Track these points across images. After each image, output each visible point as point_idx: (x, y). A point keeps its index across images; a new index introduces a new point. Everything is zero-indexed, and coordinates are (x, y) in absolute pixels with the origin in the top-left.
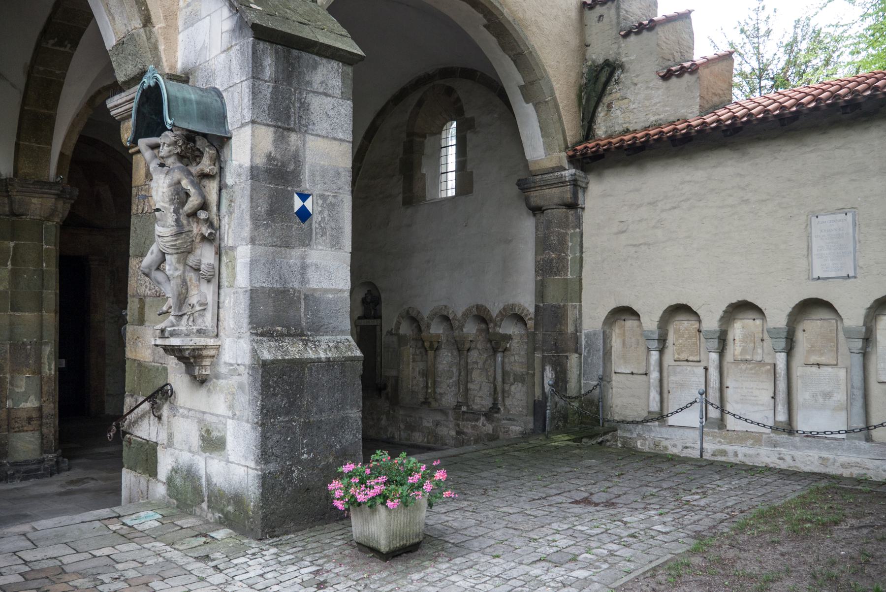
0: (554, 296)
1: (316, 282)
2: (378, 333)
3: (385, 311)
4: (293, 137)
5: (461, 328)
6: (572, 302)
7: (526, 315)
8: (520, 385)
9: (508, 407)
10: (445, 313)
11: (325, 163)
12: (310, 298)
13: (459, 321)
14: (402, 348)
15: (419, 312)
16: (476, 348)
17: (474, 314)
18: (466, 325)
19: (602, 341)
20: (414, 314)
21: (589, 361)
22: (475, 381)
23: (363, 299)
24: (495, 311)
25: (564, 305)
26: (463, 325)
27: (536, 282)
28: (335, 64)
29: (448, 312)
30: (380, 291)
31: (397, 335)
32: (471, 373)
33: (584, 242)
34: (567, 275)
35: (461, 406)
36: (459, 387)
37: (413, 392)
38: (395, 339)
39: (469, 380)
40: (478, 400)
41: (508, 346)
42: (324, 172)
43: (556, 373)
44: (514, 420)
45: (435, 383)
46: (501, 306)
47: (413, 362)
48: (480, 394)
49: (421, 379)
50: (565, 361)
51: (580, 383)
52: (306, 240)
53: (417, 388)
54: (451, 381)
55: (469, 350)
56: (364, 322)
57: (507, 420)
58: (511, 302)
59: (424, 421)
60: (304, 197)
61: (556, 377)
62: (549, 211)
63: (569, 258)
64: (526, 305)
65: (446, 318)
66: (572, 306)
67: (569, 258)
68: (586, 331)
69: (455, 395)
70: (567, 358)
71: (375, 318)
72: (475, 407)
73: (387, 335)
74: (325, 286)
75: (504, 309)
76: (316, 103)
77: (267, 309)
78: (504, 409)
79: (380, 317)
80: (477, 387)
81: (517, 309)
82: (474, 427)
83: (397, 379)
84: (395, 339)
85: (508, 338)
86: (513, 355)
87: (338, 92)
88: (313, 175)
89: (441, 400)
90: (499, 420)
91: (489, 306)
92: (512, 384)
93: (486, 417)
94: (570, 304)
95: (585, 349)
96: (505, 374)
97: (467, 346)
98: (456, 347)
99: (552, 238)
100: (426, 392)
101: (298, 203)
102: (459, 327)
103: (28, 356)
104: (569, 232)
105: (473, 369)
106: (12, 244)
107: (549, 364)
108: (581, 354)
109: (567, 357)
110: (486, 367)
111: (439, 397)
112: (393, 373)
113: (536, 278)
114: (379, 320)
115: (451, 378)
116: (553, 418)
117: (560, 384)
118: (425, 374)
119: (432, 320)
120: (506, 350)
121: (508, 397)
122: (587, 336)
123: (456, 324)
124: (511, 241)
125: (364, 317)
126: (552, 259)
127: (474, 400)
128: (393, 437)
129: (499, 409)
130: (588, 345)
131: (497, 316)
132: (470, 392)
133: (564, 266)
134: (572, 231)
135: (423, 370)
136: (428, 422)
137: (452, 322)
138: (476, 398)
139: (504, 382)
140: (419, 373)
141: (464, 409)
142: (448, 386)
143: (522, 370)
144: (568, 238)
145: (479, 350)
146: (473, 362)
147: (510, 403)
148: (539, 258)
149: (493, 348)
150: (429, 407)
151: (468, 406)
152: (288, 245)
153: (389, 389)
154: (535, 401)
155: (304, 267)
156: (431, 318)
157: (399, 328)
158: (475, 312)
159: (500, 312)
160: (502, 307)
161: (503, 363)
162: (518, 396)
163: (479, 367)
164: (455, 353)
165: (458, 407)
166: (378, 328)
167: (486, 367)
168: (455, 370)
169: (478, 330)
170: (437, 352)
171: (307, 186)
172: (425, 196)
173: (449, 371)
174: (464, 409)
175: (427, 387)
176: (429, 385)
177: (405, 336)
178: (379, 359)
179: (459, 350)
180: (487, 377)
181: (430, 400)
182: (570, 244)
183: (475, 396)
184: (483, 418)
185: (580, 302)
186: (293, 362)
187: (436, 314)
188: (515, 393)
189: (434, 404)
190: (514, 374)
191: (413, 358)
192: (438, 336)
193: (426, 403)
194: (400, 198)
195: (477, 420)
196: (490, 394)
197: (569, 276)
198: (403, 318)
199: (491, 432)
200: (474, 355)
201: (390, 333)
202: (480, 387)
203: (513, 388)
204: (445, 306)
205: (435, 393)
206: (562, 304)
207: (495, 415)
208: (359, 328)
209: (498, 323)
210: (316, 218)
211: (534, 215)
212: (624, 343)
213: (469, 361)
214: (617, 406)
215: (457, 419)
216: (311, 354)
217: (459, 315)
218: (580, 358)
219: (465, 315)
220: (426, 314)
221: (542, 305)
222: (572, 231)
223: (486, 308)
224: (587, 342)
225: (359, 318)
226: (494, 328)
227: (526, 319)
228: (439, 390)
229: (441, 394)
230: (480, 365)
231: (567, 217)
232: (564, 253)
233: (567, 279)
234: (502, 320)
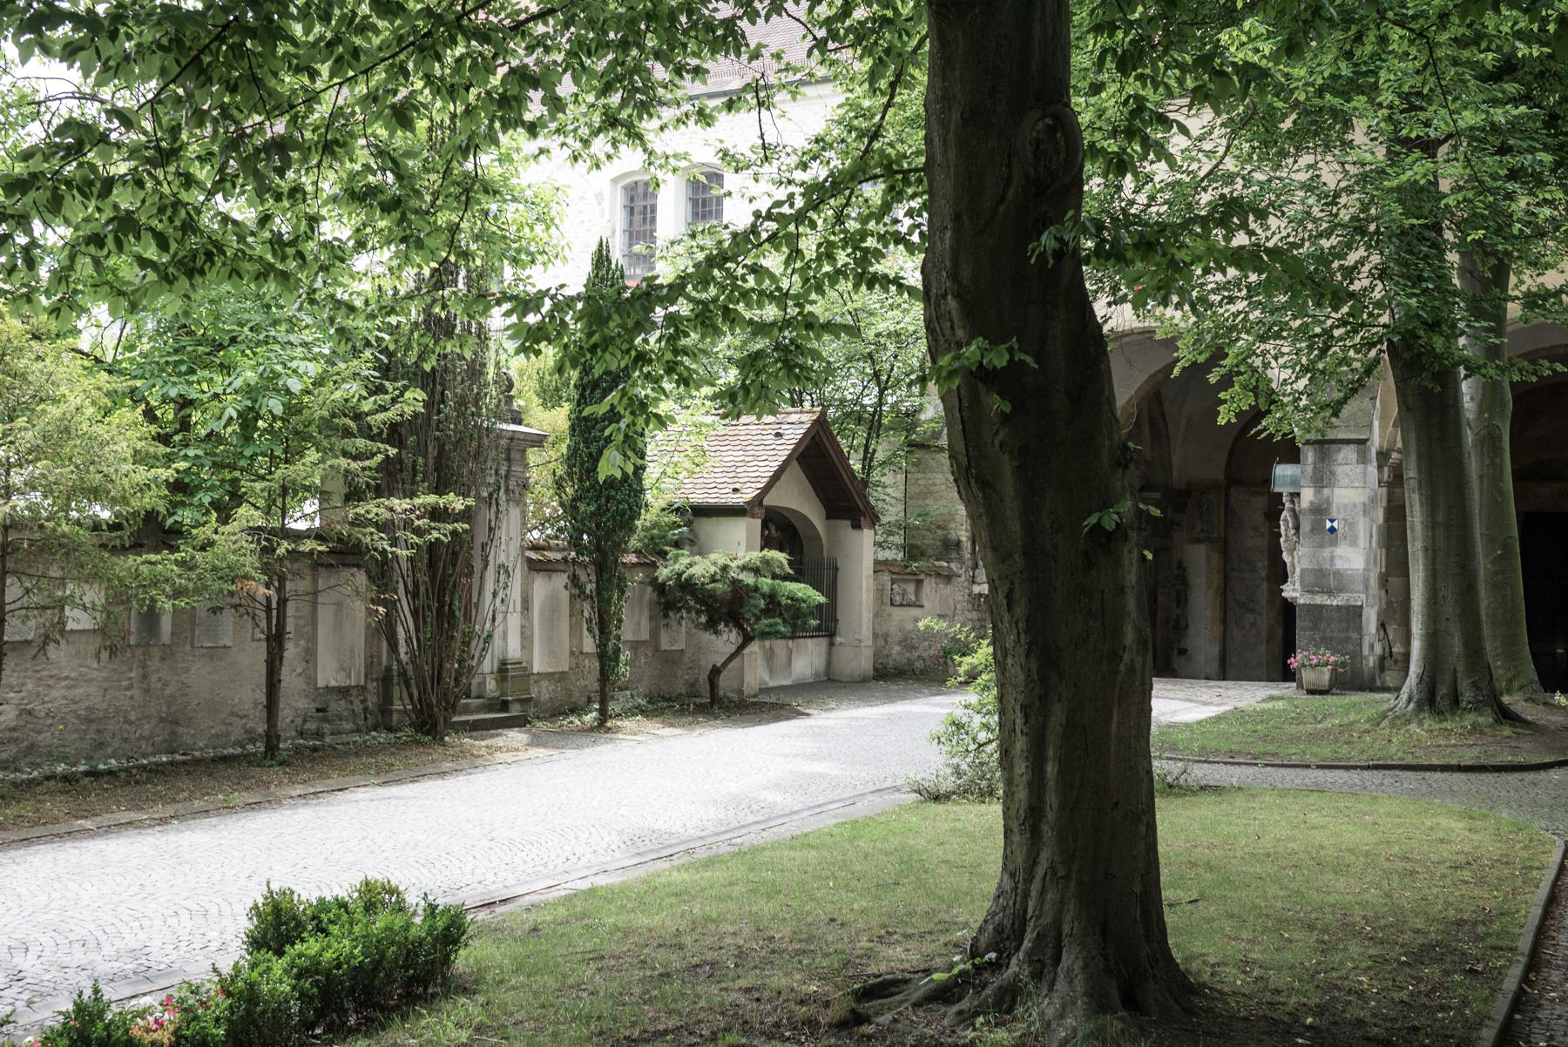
1: (1340, 565)
4: (1326, 491)
11: (1347, 501)
12: (1337, 573)
28: (1352, 446)
42: (1345, 506)
52: (1334, 543)
60: (1332, 521)
74: (1346, 567)
76: (1340, 470)
77: (1310, 579)
87: (1355, 461)
88: (1338, 509)
101: (1328, 525)
103: (1395, 612)
152: (1322, 546)
155: (1332, 558)
171: (1334, 515)
186: (1316, 606)
210: (1341, 531)
216: (1328, 602)
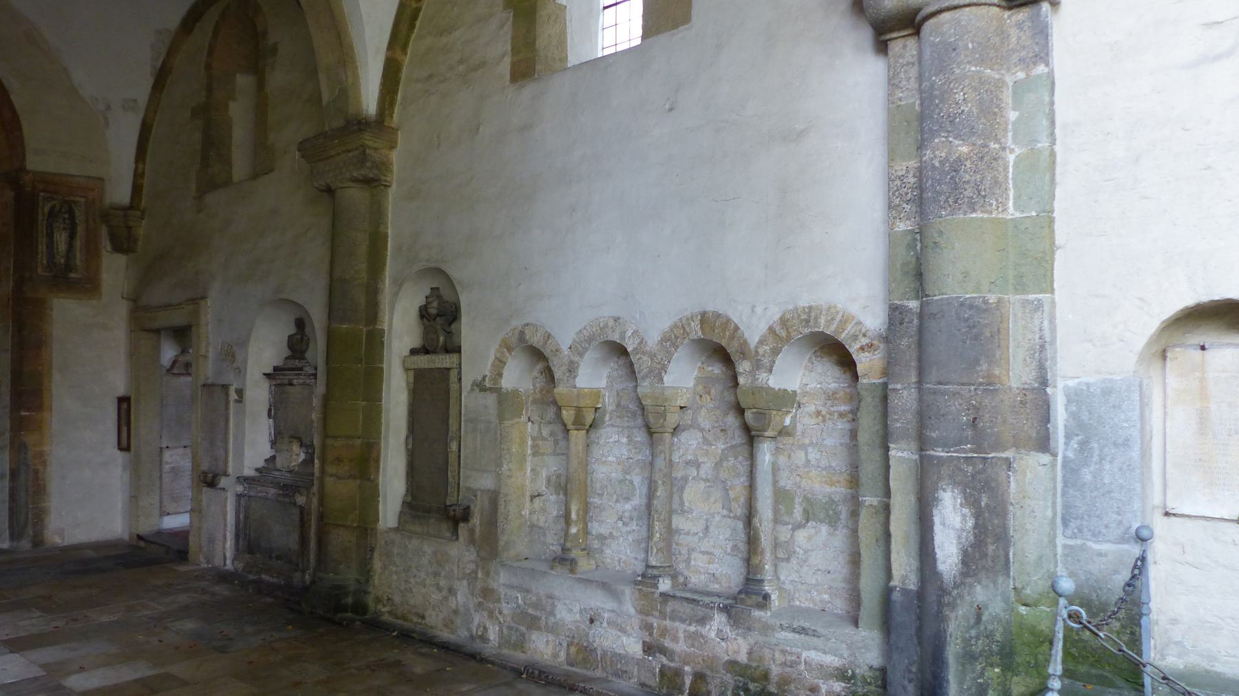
0: (966, 274)
2: (454, 386)
3: (469, 332)
5: (658, 373)
6: (1025, 292)
7: (855, 337)
8: (824, 529)
9: (788, 586)
10: (616, 337)
13: (652, 356)
14: (507, 423)
15: (549, 336)
16: (694, 425)
17: (693, 336)
18: (672, 367)
19: (1137, 413)
20: (536, 340)
21: (1087, 475)
22: (691, 511)
23: (420, 308)
24: (754, 330)
25: (1000, 301)
26: (664, 368)
27: (892, 239)
29: (623, 334)
30: (458, 289)
31: (497, 390)
32: (682, 489)
33: (1057, 107)
34: (1005, 210)
35: (656, 577)
36: (650, 528)
37: (532, 526)
38: (491, 400)
39: (675, 506)
40: (699, 561)
41: (788, 421)
43: (978, 515)
44: (815, 634)
45: (586, 508)
46: (775, 314)
47: (534, 454)
48: (706, 545)
49: (553, 498)
50: (1003, 474)
51: (1055, 546)
53: (542, 519)
54: (628, 507)
55: (676, 430)
56: (423, 361)
57: (794, 631)
58: (803, 303)
59: (559, 606)
61: (976, 526)
62: (946, 16)
63: (1011, 158)
64: (854, 309)
65: (619, 351)
66: (1025, 303)
67: (1011, 158)
68: (1071, 383)
69: (638, 542)
70: (1009, 467)
71: (447, 351)
72: (696, 580)
73: (472, 390)
75: (784, 322)
78: (780, 597)
79: (458, 350)
80: (698, 527)
81: (822, 321)
82: (693, 637)
83: (494, 498)
84: (491, 400)
85: (786, 400)
86: (803, 447)
89: (602, 551)
90: (766, 628)
91: (738, 314)
92: (799, 526)
93: (730, 616)
94: (1014, 298)
95: (1068, 437)
96: (782, 497)
97: (672, 419)
98: (640, 421)
99: (960, 97)
100: (566, 534)
102: (651, 371)
104: (1009, 80)
105: (685, 479)
107: (955, 484)
108: (1055, 455)
109: (1008, 463)
110: (723, 475)
111: (596, 544)
112: (485, 482)
113: (891, 226)
114: (455, 357)
115: (627, 499)
116: (969, 657)
117: (991, 548)
118: (564, 486)
119: (581, 355)
120: (784, 432)
121: (788, 560)
122: (1074, 397)
123: (643, 364)
124: (801, 134)
125: (424, 350)
126: (960, 161)
127: (688, 561)
128: (484, 638)
129: (766, 597)
130: (1078, 427)
131: (761, 342)
132: (682, 539)
133: (996, 182)
134: (1021, 75)
135: (559, 476)
136: (568, 613)
137: (633, 359)
138: (694, 555)
139: (776, 521)
140: (549, 480)
141: (665, 585)
142: (620, 519)
143: (828, 489)
144: (1007, 96)
145: (702, 430)
146: (688, 463)
147: (794, 577)
148: (901, 167)
149: (747, 429)
150: (572, 571)
151: (674, 577)
153: (476, 520)
154: (887, 592)
156: (579, 349)
157: (500, 375)
158: (696, 331)
159: (771, 330)
160: (777, 317)
161: (775, 469)
162: (817, 559)
163: (703, 474)
164: (640, 436)
165: (647, 578)
166: (453, 375)
167: (723, 475)
168: (637, 479)
169: (698, 380)
170: (593, 435)
172: (564, 59)
173: (621, 482)
174: (665, 585)
175: (567, 517)
176: (574, 516)
177: (515, 393)
178: (454, 446)
179: (650, 432)
180: (727, 503)
181: (575, 553)
182: (1013, 116)
183: (691, 550)
184: (719, 620)
185: (1052, 291)
187: (590, 340)
188: (806, 552)
189: (585, 565)
190: (806, 499)
191: (533, 447)
192: (597, 394)
193: (563, 560)
194: (505, 67)
195: (703, 621)
196: (735, 547)
197: (1012, 212)
198: (510, 350)
199: (743, 658)
200: (689, 444)
201: (480, 386)
202: (707, 528)
203: (801, 536)
204: (616, 319)
205: (586, 532)
206: (992, 299)
207: (757, 613)
208: (411, 373)
209: (766, 361)
211: (882, 47)
212: (1203, 420)
213: (676, 458)
214: (1174, 621)
215: (643, 612)
217: (653, 339)
218: (1054, 465)
219: (671, 340)
220: (565, 338)
221: (913, 304)
222: (1021, 75)
223: (729, 321)
224: (1073, 416)
225: (414, 352)
226: (752, 373)
227: (853, 349)
228: (595, 528)
229: (602, 538)
230: (707, 469)
231: (1002, 33)
232: (997, 141)
233: (1005, 221)
234: (776, 352)
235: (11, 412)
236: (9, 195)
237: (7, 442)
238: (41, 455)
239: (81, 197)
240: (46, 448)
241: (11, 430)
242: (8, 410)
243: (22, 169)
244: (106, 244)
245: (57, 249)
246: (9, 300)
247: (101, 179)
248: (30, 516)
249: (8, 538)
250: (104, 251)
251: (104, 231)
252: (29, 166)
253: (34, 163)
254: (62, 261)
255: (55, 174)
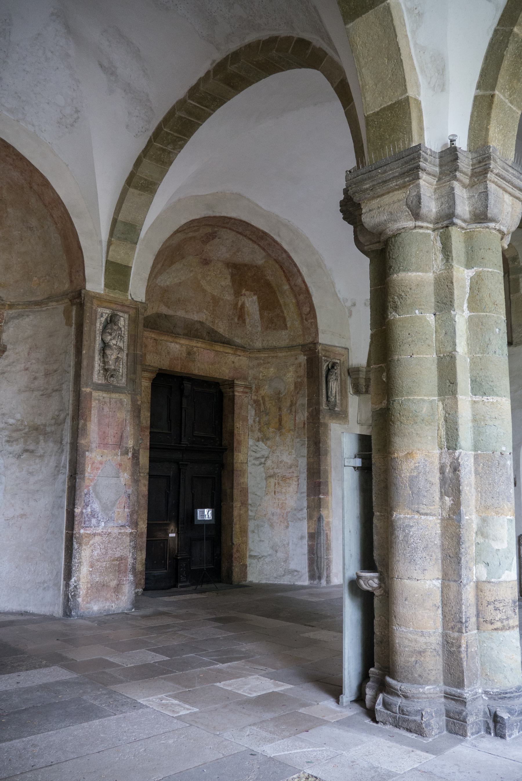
106: (471, 273)
235: (308, 496)
236: (303, 359)
237: (305, 515)
238: (328, 523)
239: (338, 359)
240: (330, 520)
241: (308, 507)
242: (305, 494)
243: (315, 343)
244: (350, 390)
245: (331, 392)
246: (304, 424)
247: (347, 349)
248: (325, 564)
249: (308, 578)
250: (349, 394)
251: (349, 381)
252: (320, 341)
253: (323, 339)
254: (333, 399)
255: (330, 346)
